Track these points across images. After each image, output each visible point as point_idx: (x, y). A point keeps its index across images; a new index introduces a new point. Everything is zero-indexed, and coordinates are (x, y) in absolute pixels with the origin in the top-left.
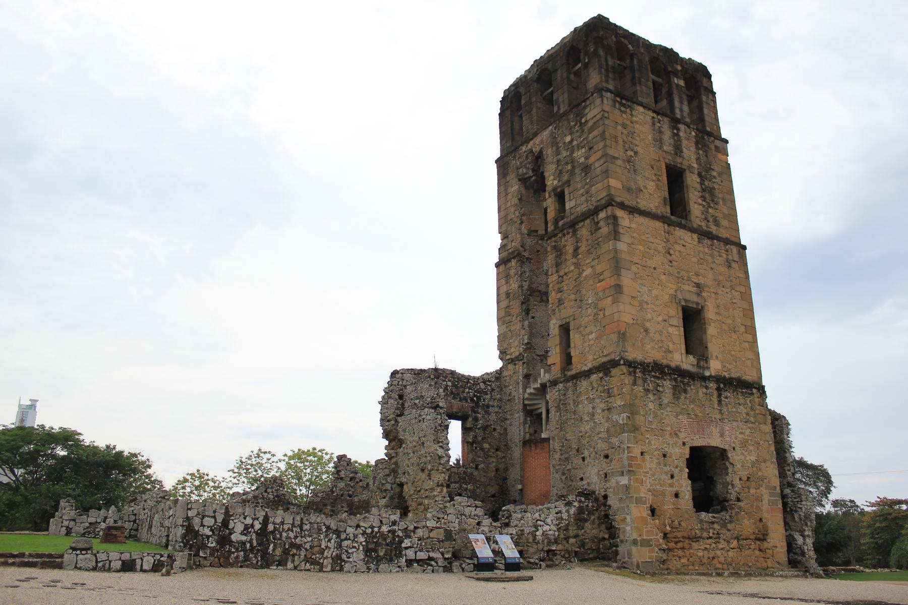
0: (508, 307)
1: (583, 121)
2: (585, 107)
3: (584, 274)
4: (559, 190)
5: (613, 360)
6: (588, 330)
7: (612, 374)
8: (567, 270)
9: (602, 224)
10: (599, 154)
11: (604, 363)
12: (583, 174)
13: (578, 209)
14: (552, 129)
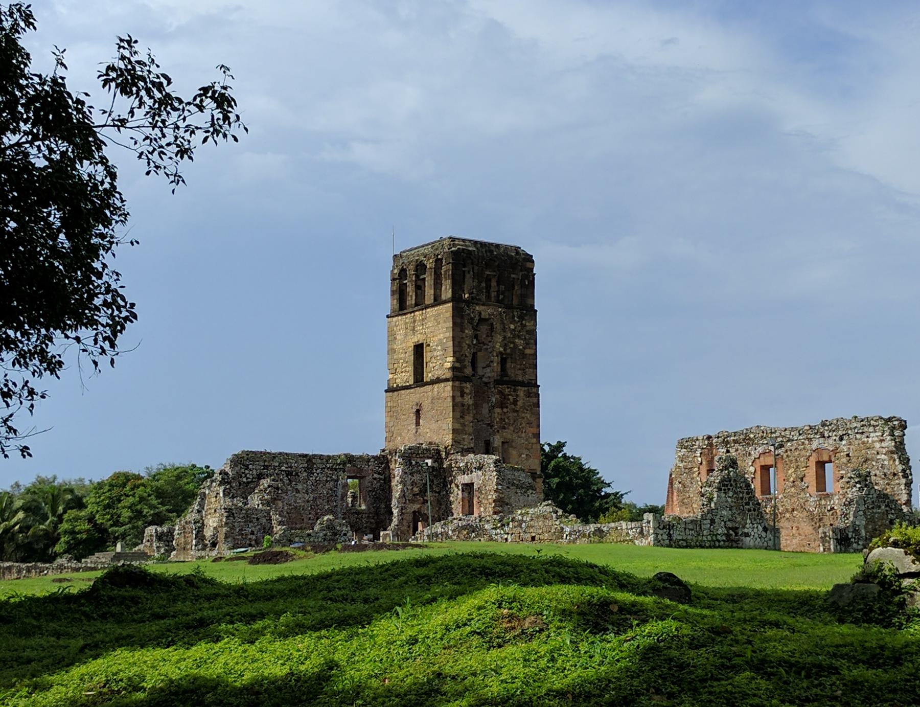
1: (524, 322)
2: (526, 314)
10: (532, 352)
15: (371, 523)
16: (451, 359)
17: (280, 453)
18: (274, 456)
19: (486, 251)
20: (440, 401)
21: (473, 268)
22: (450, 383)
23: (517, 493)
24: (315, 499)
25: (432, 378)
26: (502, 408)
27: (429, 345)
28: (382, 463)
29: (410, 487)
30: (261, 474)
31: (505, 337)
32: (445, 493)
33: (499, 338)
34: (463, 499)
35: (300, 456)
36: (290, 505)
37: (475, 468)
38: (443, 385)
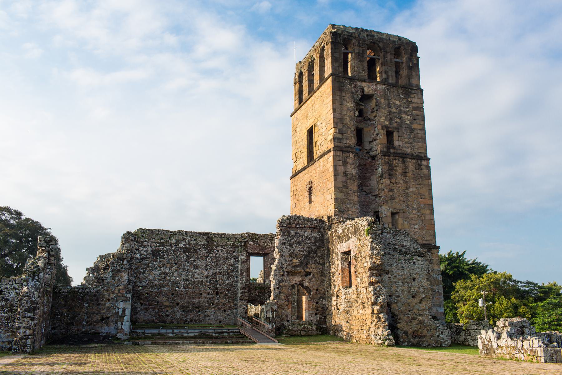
0: (346, 182)
1: (409, 99)
2: (411, 93)
3: (411, 190)
4: (390, 129)
5: (431, 245)
6: (414, 222)
7: (432, 252)
8: (397, 181)
9: (423, 167)
10: (420, 127)
11: (425, 244)
12: (409, 131)
13: (405, 149)
14: (385, 88)
16: (332, 131)
17: (179, 232)
18: (171, 234)
19: (367, 35)
22: (332, 153)
23: (399, 260)
24: (214, 275)
26: (390, 179)
30: (156, 251)
31: (390, 112)
35: (200, 234)
36: (187, 280)
37: (351, 234)
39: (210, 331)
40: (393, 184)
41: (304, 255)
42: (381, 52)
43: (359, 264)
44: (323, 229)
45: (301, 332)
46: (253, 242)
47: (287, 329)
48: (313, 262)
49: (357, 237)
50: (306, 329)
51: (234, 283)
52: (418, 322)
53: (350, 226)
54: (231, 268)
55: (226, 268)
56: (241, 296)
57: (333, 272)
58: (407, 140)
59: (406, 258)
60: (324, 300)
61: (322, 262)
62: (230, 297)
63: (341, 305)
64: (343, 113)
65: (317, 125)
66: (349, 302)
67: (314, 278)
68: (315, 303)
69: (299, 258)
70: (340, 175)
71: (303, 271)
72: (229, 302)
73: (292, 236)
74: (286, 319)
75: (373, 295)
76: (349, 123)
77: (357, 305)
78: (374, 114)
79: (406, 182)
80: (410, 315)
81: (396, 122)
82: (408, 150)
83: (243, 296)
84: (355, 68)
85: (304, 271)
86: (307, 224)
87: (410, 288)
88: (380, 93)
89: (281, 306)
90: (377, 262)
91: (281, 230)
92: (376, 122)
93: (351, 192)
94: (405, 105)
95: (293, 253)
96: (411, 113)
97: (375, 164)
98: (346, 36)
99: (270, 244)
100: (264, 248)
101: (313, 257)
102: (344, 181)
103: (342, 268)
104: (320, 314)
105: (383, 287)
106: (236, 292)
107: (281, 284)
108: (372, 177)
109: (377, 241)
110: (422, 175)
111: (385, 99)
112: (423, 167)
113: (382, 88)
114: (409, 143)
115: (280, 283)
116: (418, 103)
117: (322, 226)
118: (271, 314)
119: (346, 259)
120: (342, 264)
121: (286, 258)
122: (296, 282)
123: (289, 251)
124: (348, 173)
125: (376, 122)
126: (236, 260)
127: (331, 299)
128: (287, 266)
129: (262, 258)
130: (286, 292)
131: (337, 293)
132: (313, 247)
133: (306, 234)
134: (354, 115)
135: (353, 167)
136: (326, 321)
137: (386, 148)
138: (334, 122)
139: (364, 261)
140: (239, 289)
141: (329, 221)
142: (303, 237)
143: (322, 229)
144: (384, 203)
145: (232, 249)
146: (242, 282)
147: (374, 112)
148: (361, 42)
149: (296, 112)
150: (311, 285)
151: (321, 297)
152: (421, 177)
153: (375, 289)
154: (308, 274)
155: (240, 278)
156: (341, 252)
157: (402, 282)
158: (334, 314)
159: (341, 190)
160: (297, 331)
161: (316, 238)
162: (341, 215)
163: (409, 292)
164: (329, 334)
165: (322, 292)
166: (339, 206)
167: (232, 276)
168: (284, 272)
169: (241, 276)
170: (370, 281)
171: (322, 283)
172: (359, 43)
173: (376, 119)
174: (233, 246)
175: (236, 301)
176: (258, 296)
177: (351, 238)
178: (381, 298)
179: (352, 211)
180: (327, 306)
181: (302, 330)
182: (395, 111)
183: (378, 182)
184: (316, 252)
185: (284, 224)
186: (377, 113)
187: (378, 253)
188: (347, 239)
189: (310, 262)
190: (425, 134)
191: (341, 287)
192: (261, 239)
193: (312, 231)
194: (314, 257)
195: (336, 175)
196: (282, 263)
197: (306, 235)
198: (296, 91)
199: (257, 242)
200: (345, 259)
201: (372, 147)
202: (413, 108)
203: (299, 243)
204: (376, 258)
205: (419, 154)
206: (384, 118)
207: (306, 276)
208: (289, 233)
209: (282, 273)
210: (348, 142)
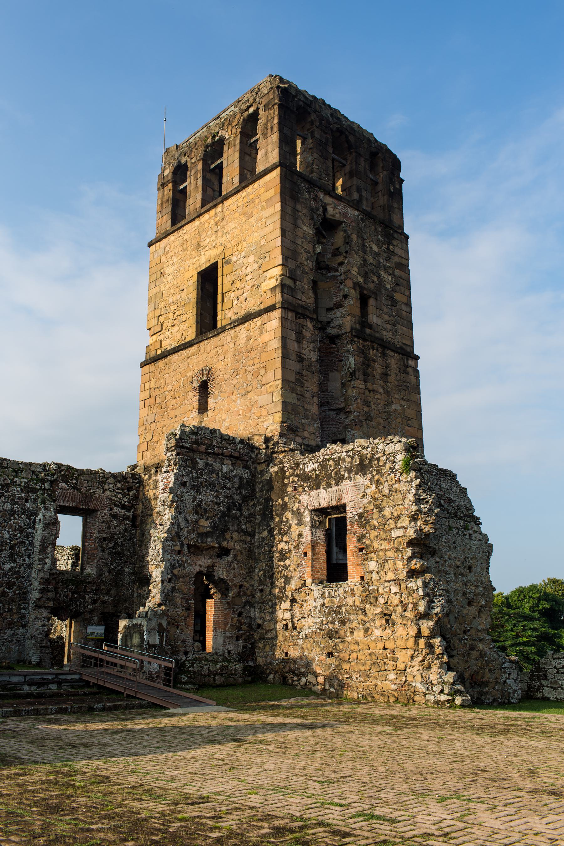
3: (394, 407)
4: (365, 292)
8: (375, 389)
13: (384, 333)
15: (104, 602)
16: (278, 271)
20: (253, 354)
21: (312, 134)
22: (277, 314)
25: (234, 317)
26: (365, 381)
27: (228, 262)
28: (129, 489)
29: (191, 517)
32: (265, 533)
33: (355, 260)
34: (314, 545)
37: (349, 471)
38: (258, 321)
39: (15, 679)
40: (370, 391)
41: (220, 512)
42: (351, 153)
43: (374, 533)
44: (253, 463)
45: (216, 678)
46: (66, 483)
47: (190, 671)
48: (236, 528)
49: (369, 476)
50: (224, 672)
51: (22, 569)
52: (478, 653)
53: (344, 454)
54: (19, 535)
55: (7, 535)
56: (39, 600)
57: (282, 549)
58: (387, 317)
59: (459, 525)
60: (252, 609)
61: (250, 530)
62: (13, 601)
63: (303, 620)
64: (296, 242)
65: (231, 260)
66: (337, 612)
67: (236, 562)
68: (236, 616)
69: (211, 518)
70: (291, 358)
71: (217, 546)
72: (10, 610)
73: (200, 469)
74: (182, 649)
75: (423, 598)
76: (306, 263)
77: (366, 619)
78: (341, 259)
79: (388, 392)
80: (467, 640)
81: (373, 282)
82: (388, 336)
83: (42, 599)
84: (315, 166)
85: (220, 545)
86: (227, 448)
87: (466, 585)
88: (351, 222)
89: (174, 619)
90: (427, 530)
91: (178, 454)
92: (341, 275)
93: (308, 395)
94: (385, 255)
95: (199, 505)
96: (393, 272)
97: (338, 351)
98: (301, 103)
99: (100, 491)
100: (88, 497)
101: (235, 518)
102: (298, 371)
103: (312, 541)
104: (243, 638)
105: (440, 580)
106: (25, 588)
107: (176, 572)
108: (330, 374)
109: (427, 484)
110: (408, 385)
111: (358, 236)
112: (409, 370)
113: (354, 215)
114: (390, 323)
115: (174, 568)
116: (402, 258)
117: (251, 456)
118: (158, 637)
119: (321, 523)
120: (312, 533)
121: (187, 515)
122: (201, 569)
123: (193, 501)
124: (305, 357)
125: (341, 275)
126: (30, 519)
127: (274, 606)
128: (188, 532)
129: (78, 521)
130: (185, 589)
131: (292, 595)
132: (236, 497)
133: (225, 468)
134: (314, 251)
135: (311, 348)
136: (254, 653)
137: (359, 324)
138: (282, 255)
139: (393, 526)
140: (36, 584)
141: (267, 448)
142: (218, 473)
143: (250, 463)
144: (356, 425)
145: (23, 495)
146: (43, 568)
147: (340, 254)
148: (323, 122)
149: (160, 240)
150: (231, 576)
151: (248, 603)
152: (407, 387)
153: (425, 584)
154: (224, 552)
155: (39, 560)
156: (310, 508)
157: (455, 574)
158: (280, 638)
159: (293, 388)
160: (209, 676)
161: (241, 478)
162: (292, 436)
163: (464, 594)
164: (266, 681)
165: (249, 592)
166: (288, 419)
167: (20, 555)
168: (182, 545)
169: (40, 555)
170: (411, 569)
171: (250, 572)
172: (321, 123)
173: (342, 269)
174: (26, 489)
175: (24, 608)
176: (71, 600)
177: (350, 478)
178: (437, 603)
179: (309, 432)
180: (260, 622)
181: (217, 674)
182: (371, 261)
183: (343, 385)
184: (240, 509)
185: (185, 442)
186: (346, 257)
187: (430, 509)
188: (332, 482)
189: (231, 528)
190: (410, 313)
191: (309, 581)
192: (83, 478)
193: (232, 464)
194: (237, 518)
195: (285, 357)
196: (179, 525)
197: (224, 471)
198: (165, 199)
199: (76, 484)
200: (320, 524)
201: (332, 320)
202: (395, 264)
203: (212, 485)
204: (425, 521)
205: (404, 347)
206: (356, 269)
207: (220, 556)
208: (194, 463)
209: (178, 548)
210: (304, 298)
